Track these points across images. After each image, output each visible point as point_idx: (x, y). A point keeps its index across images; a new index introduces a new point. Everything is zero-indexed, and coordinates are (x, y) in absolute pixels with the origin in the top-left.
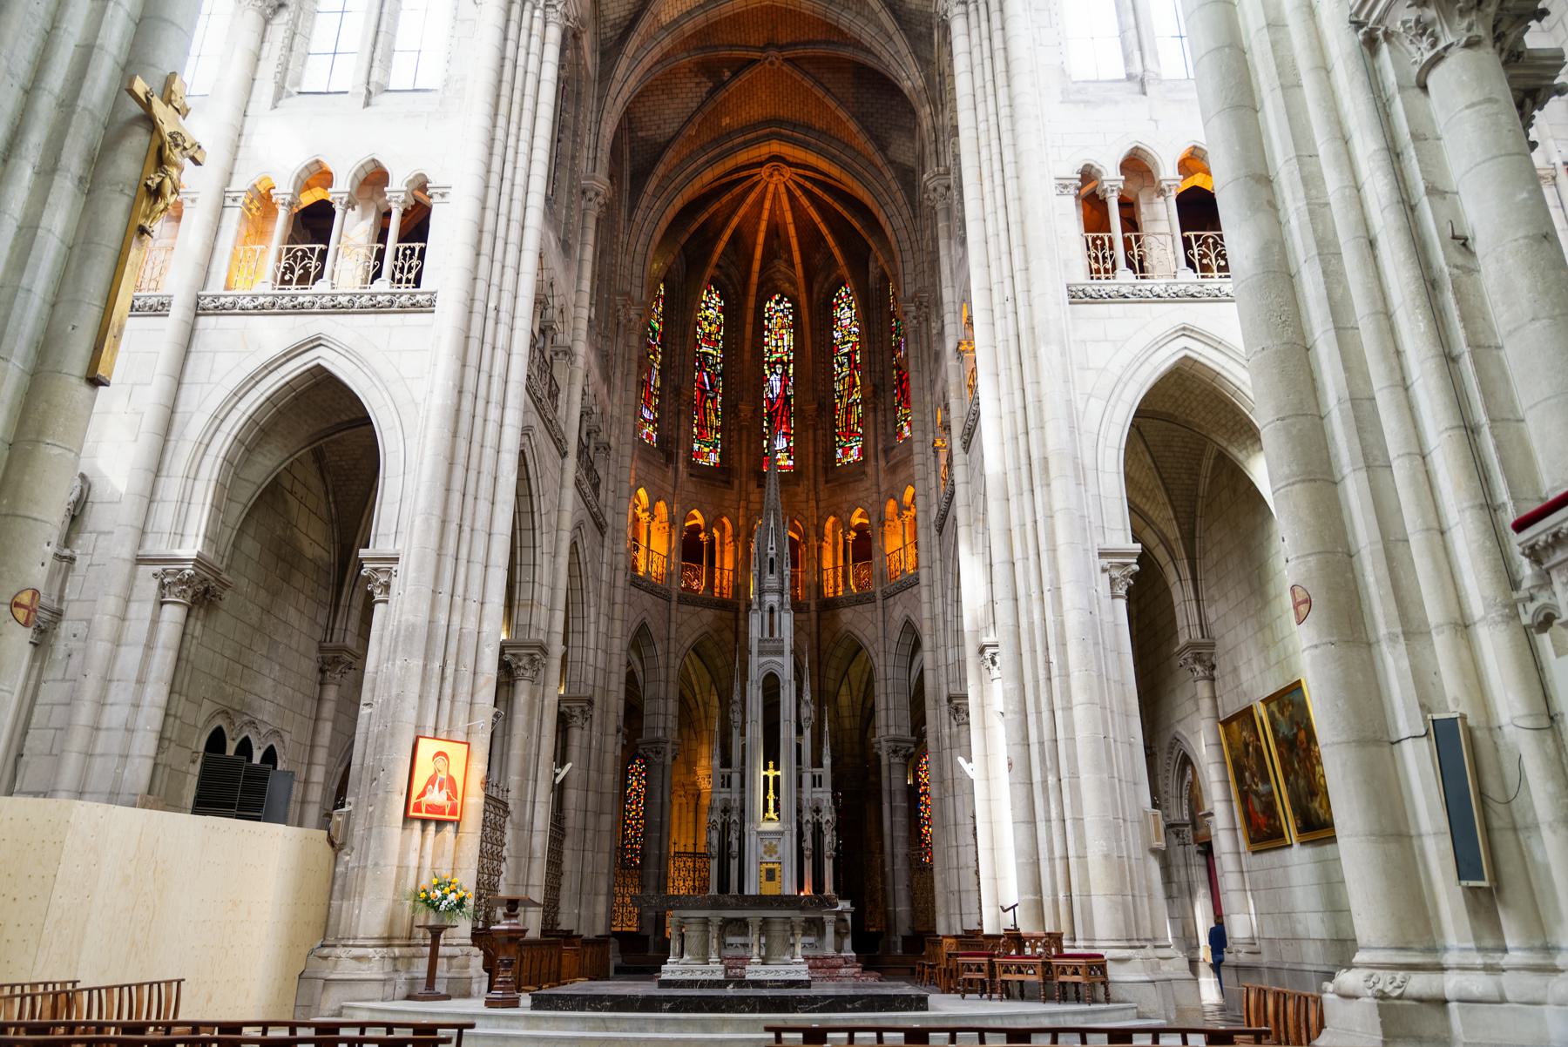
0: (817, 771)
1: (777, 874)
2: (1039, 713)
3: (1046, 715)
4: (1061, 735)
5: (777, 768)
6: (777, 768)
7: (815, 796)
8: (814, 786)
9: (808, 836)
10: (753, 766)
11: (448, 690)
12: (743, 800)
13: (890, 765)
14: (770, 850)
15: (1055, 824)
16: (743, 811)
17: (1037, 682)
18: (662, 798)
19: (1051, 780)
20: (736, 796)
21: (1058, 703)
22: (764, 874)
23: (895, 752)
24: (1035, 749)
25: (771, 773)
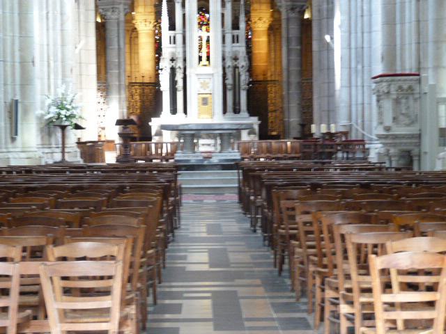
0: (236, 32)
1: (209, 101)
2: (356, 33)
3: (359, 35)
4: (366, 45)
5: (207, 31)
6: (207, 31)
7: (234, 49)
8: (233, 42)
9: (229, 76)
10: (191, 31)
11: (51, 25)
12: (185, 52)
13: (288, 19)
14: (204, 85)
15: (360, 88)
16: (185, 60)
17: (356, 16)
18: (119, 45)
19: (360, 67)
20: (180, 50)
21: (366, 29)
22: (201, 101)
23: (292, 9)
24: (353, 51)
25: (204, 35)
